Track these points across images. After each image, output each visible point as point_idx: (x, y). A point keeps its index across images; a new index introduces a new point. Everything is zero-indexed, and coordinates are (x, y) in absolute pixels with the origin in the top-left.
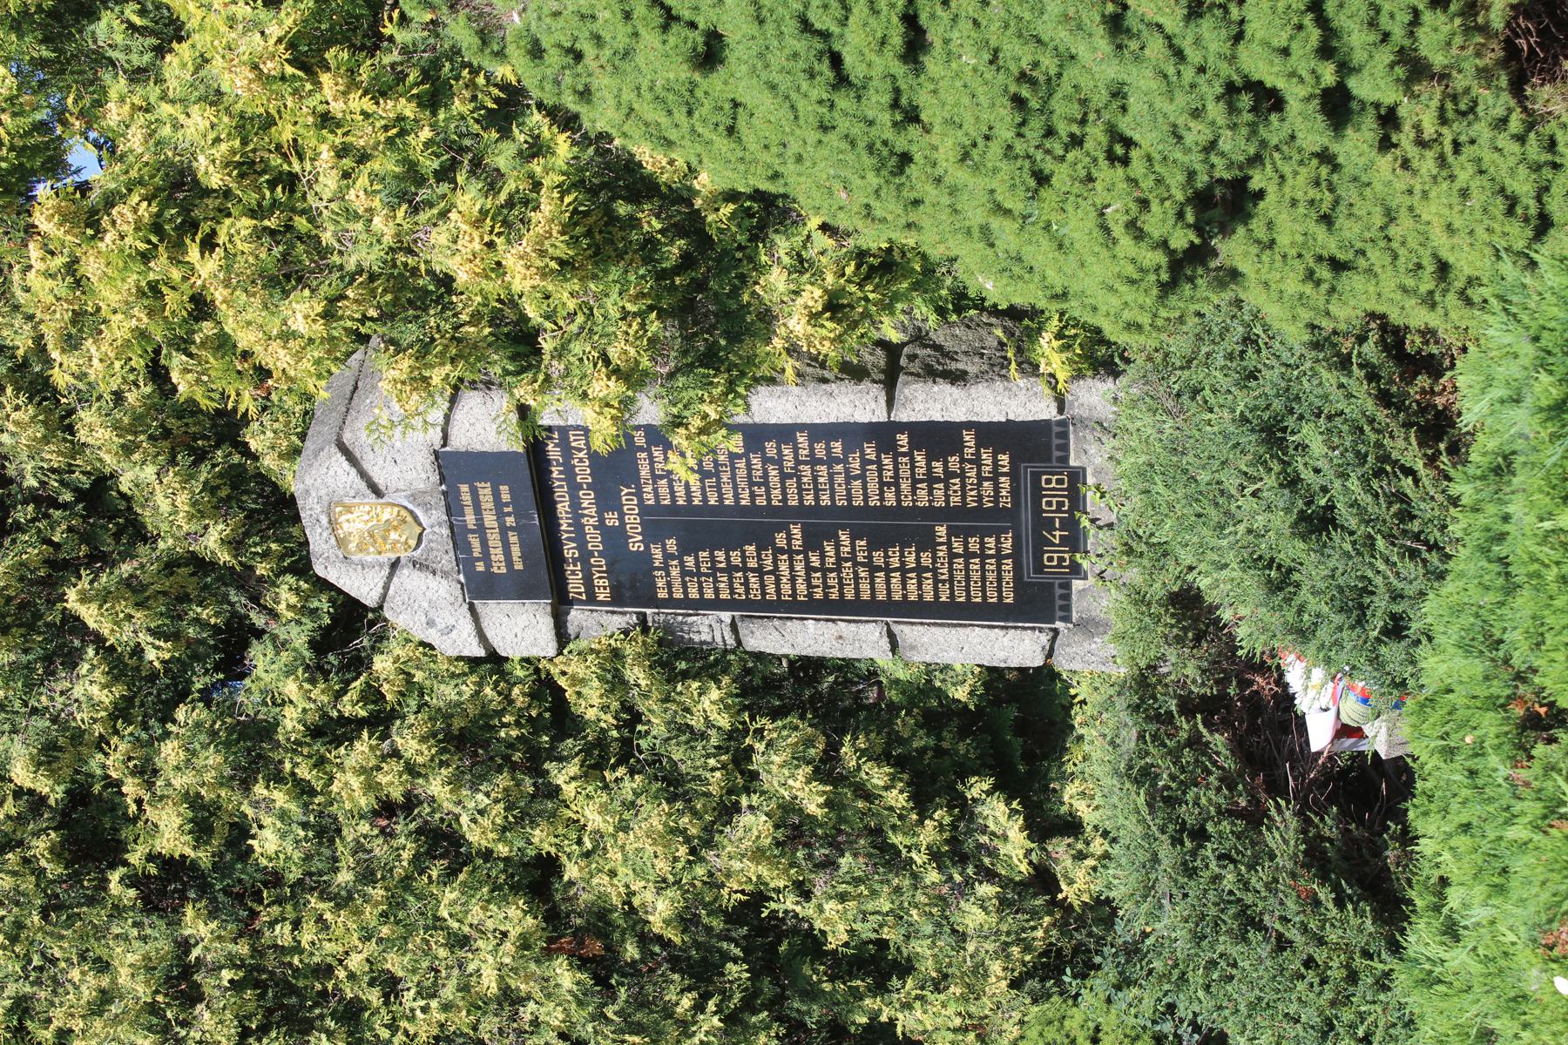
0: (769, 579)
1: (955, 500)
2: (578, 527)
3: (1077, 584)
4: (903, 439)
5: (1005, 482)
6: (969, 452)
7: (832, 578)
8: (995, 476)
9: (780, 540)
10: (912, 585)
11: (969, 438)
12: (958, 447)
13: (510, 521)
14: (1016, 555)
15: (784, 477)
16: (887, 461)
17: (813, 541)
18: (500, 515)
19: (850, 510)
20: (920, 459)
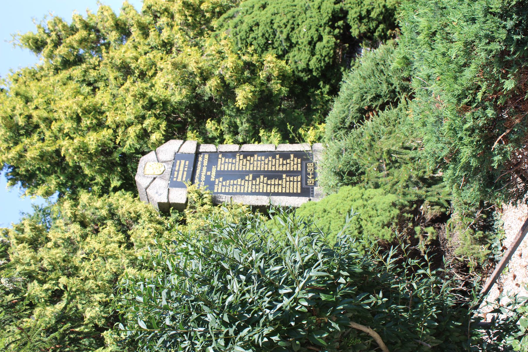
0: (242, 187)
1: (288, 169)
2: (200, 175)
3: (315, 188)
4: (278, 156)
5: (299, 165)
6: (292, 159)
7: (257, 187)
8: (297, 163)
9: (247, 178)
10: (276, 188)
11: (292, 156)
12: (289, 158)
13: (186, 169)
14: (301, 181)
15: (250, 164)
16: (274, 160)
17: (254, 178)
18: (184, 167)
19: (264, 171)
20: (281, 160)
